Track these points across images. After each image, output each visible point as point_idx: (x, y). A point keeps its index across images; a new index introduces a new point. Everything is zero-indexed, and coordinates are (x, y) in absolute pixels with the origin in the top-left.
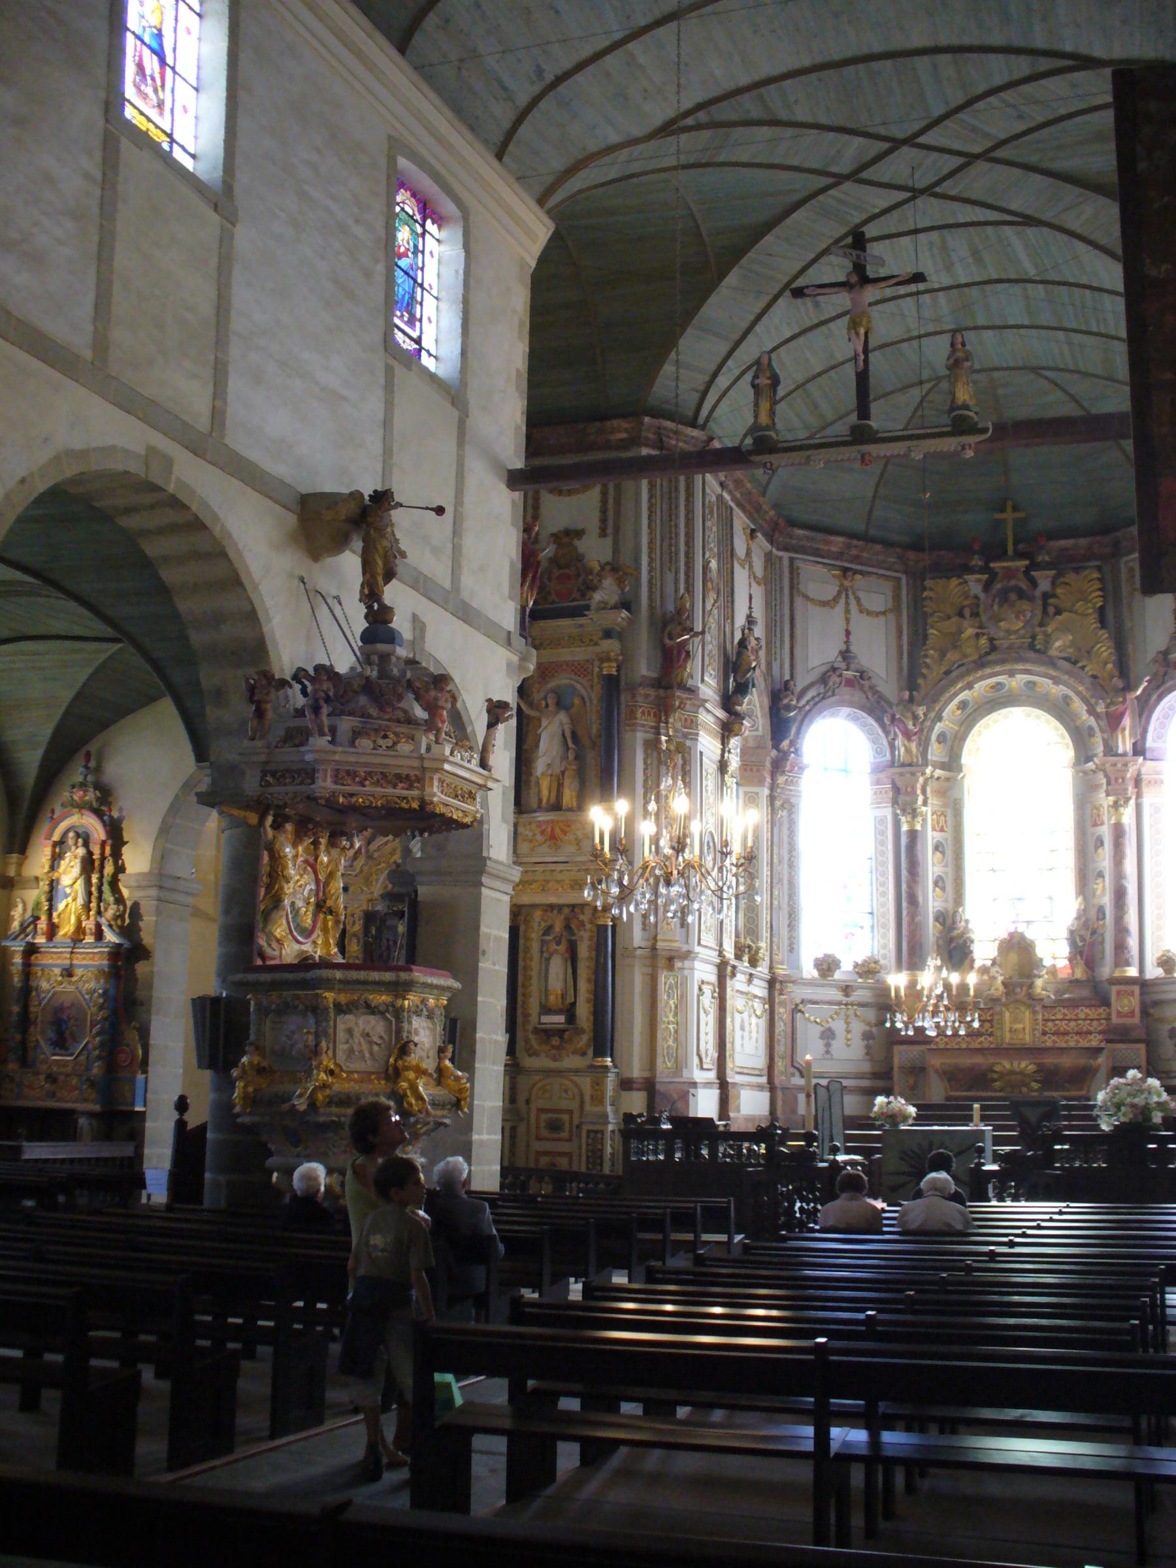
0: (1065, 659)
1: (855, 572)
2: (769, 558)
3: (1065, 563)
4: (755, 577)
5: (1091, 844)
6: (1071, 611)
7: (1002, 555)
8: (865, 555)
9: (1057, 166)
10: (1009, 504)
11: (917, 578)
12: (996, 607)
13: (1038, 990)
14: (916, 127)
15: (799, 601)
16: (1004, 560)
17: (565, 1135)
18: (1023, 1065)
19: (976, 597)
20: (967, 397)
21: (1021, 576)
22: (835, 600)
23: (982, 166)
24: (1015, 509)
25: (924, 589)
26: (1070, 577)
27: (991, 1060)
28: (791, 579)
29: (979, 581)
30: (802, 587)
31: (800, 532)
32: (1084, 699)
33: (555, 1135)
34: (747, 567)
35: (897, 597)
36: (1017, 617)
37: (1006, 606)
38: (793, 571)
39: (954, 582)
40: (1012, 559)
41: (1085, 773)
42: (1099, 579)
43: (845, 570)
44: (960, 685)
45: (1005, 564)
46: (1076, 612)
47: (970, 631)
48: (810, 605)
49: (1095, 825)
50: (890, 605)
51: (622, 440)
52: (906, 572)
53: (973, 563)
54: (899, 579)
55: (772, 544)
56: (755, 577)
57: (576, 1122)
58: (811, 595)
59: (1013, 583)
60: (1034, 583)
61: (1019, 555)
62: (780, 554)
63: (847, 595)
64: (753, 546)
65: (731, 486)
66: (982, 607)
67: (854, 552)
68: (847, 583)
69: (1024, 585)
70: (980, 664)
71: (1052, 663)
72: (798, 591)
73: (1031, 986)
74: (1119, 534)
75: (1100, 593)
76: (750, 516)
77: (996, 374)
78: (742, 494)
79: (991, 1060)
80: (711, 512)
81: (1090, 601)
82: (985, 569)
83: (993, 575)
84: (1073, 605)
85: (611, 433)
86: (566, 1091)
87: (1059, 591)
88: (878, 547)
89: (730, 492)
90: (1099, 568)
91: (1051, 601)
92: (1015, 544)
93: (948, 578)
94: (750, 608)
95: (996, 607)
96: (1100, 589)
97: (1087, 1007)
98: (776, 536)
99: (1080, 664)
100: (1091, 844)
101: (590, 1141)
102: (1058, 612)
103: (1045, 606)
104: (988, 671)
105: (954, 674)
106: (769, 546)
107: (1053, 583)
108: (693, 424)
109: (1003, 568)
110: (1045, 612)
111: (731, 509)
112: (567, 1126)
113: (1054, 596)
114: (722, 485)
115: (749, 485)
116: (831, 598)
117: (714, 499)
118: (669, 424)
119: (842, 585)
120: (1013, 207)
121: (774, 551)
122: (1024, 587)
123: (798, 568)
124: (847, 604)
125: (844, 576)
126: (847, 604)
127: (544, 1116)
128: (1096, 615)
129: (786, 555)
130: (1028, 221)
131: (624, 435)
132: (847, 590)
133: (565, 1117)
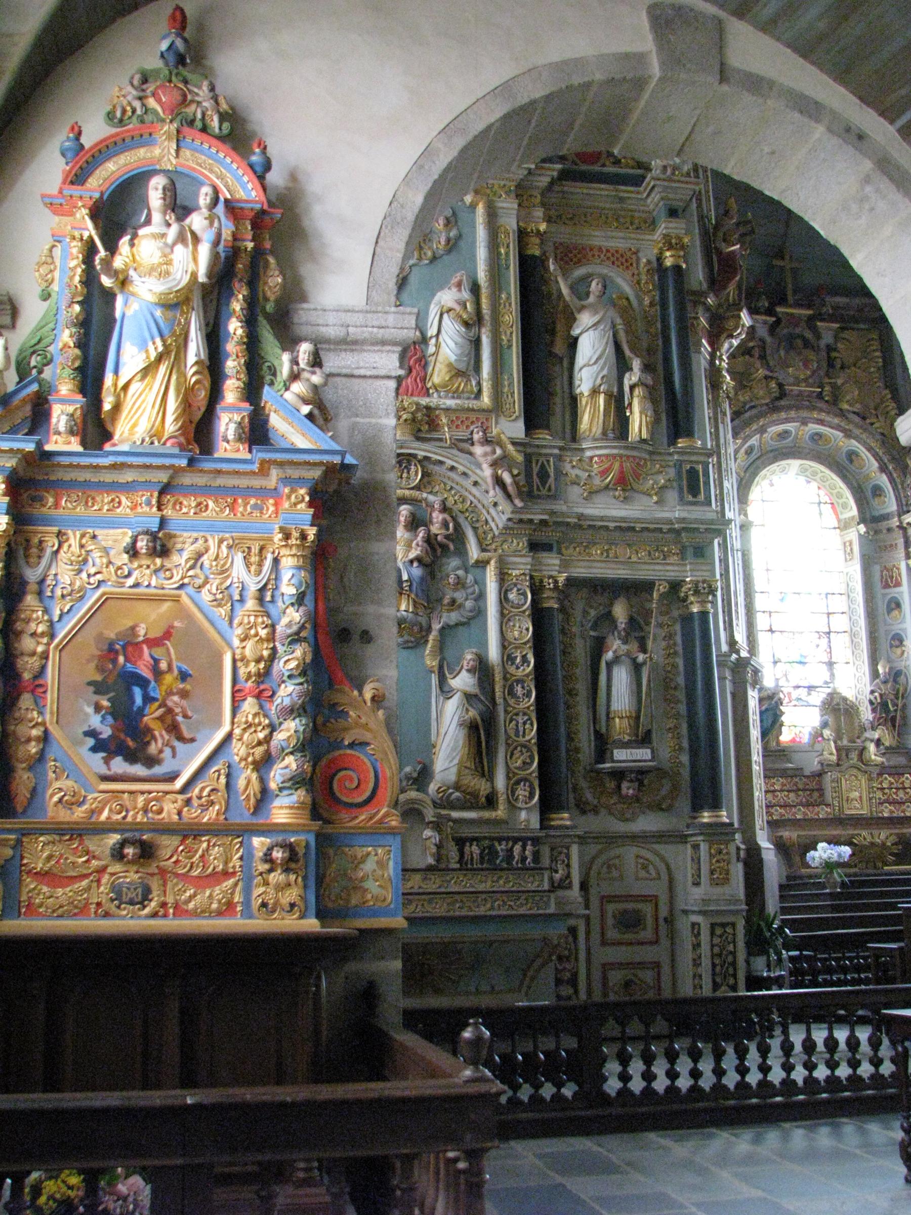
0: (854, 413)
5: (882, 607)
7: (783, 301)
12: (782, 353)
13: (873, 757)
17: (647, 934)
18: (883, 836)
19: (762, 340)
21: (803, 324)
27: (851, 832)
32: (876, 456)
33: (629, 936)
36: (806, 365)
40: (791, 306)
41: (876, 532)
44: (755, 427)
47: (762, 372)
49: (887, 586)
57: (663, 912)
59: (798, 331)
60: (818, 337)
69: (808, 335)
70: (774, 407)
71: (842, 414)
73: (863, 750)
79: (851, 832)
82: (770, 312)
86: (645, 868)
91: (834, 354)
97: (890, 775)
99: (868, 421)
100: (882, 607)
101: (716, 940)
102: (842, 368)
104: (783, 415)
105: (747, 415)
107: (836, 338)
109: (787, 313)
110: (831, 364)
112: (650, 921)
113: (835, 350)
127: (611, 908)
133: (647, 909)
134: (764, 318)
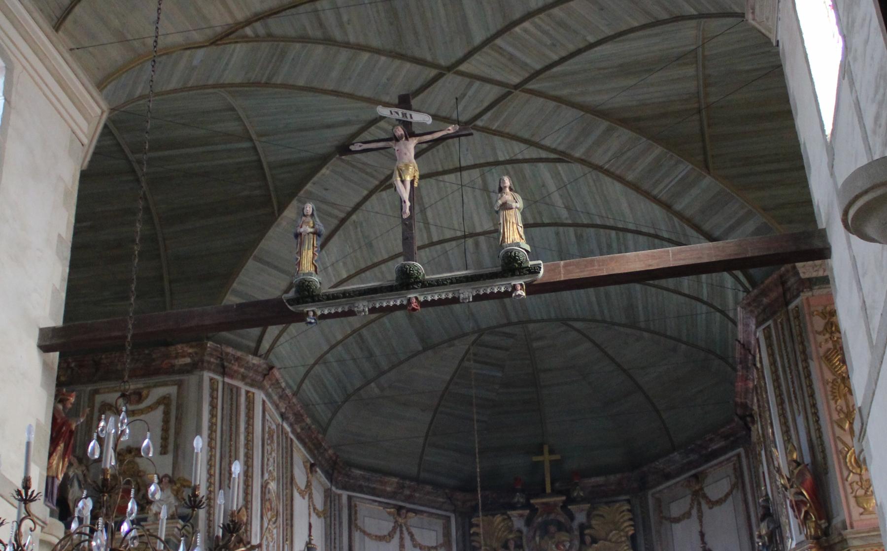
1: (409, 510)
2: (328, 494)
3: (599, 497)
4: (315, 509)
6: (606, 540)
7: (542, 492)
8: (417, 495)
9: (589, 99)
10: (546, 449)
11: (466, 516)
12: (537, 539)
14: (460, 54)
15: (357, 535)
16: (542, 497)
19: (520, 531)
20: (517, 237)
21: (559, 509)
22: (391, 535)
23: (520, 97)
24: (551, 452)
25: (472, 525)
26: (603, 510)
28: (350, 515)
29: (521, 516)
30: (359, 523)
31: (358, 472)
34: (307, 497)
35: (447, 534)
37: (546, 538)
38: (352, 508)
39: (498, 518)
40: (550, 495)
42: (629, 510)
43: (399, 509)
45: (544, 500)
46: (610, 541)
48: (367, 539)
50: (441, 541)
51: (186, 365)
52: (454, 511)
53: (516, 500)
54: (449, 517)
55: (331, 482)
56: (315, 509)
58: (367, 530)
59: (552, 517)
60: (572, 517)
61: (556, 492)
62: (339, 492)
63: (401, 532)
64: (314, 483)
65: (292, 418)
66: (524, 540)
67: (407, 492)
68: (400, 520)
69: (562, 518)
72: (356, 526)
74: (645, 469)
75: (631, 523)
76: (310, 451)
77: (531, 326)
78: (302, 429)
80: (271, 437)
81: (623, 530)
82: (527, 505)
83: (534, 510)
84: (607, 535)
85: (176, 357)
87: (593, 522)
88: (429, 488)
89: (291, 425)
90: (629, 501)
91: (587, 531)
92: (552, 483)
93: (494, 515)
94: (310, 535)
95: (537, 539)
96: (630, 519)
98: (335, 475)
102: (594, 541)
103: (582, 535)
106: (329, 484)
107: (589, 516)
108: (255, 353)
109: (543, 504)
110: (582, 542)
111: (291, 440)
113: (590, 527)
114: (282, 416)
115: (308, 421)
116: (386, 533)
117: (274, 427)
118: (230, 350)
119: (396, 522)
120: (547, 142)
121: (334, 489)
122: (563, 520)
123: (356, 506)
124: (402, 538)
125: (399, 515)
126: (402, 538)
128: (628, 543)
129: (345, 494)
130: (563, 157)
131: (188, 360)
132: (401, 526)
134: (520, 512)
